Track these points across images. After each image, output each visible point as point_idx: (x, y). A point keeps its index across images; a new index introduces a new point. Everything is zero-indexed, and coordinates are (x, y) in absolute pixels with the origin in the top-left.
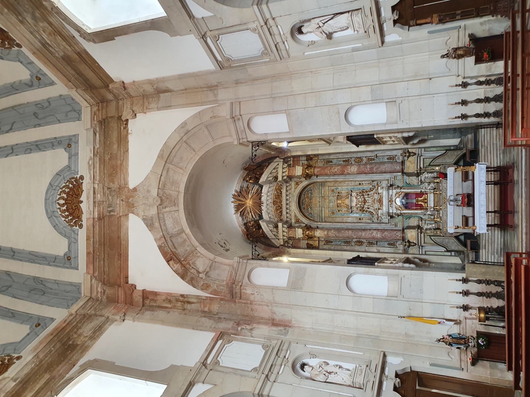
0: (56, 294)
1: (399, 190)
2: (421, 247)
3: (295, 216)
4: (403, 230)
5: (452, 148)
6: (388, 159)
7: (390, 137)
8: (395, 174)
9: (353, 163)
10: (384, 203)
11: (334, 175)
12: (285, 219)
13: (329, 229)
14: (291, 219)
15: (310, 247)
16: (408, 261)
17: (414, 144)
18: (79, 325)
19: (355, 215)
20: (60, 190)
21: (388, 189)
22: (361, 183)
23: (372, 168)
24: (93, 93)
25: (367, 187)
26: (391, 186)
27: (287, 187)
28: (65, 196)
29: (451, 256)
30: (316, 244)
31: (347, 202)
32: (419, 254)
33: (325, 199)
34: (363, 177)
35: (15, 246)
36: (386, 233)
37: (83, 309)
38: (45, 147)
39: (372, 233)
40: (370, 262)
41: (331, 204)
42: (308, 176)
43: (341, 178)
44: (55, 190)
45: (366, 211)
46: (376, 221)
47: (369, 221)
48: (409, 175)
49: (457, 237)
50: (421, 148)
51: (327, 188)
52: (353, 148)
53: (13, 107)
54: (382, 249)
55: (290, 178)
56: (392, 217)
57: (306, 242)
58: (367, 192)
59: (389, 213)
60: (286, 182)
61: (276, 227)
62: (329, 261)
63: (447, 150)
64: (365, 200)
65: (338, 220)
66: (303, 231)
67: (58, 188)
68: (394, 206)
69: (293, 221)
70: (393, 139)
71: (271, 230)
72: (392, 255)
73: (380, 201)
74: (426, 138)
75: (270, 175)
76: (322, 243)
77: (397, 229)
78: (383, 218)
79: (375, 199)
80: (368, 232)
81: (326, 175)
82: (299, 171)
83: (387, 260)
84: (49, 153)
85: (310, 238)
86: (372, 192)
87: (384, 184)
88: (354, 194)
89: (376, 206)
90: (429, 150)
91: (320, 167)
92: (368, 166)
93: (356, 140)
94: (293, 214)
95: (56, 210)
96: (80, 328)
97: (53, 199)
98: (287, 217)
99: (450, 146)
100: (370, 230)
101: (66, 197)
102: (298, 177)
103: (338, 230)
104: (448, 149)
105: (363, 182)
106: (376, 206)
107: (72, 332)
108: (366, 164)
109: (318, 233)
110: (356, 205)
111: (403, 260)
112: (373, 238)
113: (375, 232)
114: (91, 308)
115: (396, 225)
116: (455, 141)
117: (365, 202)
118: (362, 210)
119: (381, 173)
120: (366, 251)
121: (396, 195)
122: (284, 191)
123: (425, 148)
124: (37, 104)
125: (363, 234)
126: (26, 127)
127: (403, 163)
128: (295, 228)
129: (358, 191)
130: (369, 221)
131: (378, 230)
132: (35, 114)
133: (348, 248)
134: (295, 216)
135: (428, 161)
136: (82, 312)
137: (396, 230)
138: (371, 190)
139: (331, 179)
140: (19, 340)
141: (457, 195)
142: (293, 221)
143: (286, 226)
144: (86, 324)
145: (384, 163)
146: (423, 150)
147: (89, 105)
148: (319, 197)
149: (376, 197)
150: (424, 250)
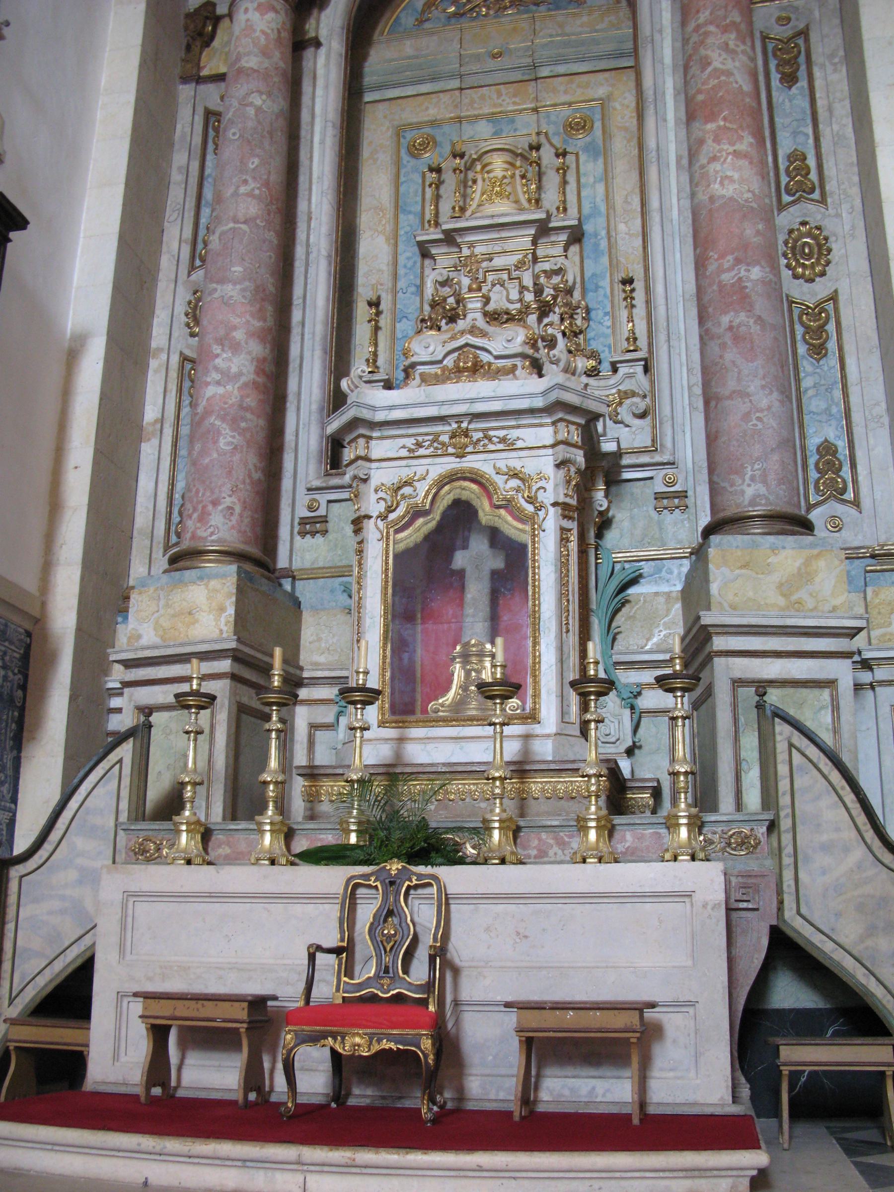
1: (552, 488)
21: (557, 408)
23: (739, 296)
25: (607, 332)
39: (235, 348)
41: (483, 129)
65: (376, 185)
68: (419, 467)
77: (284, 531)
92: (756, 273)
115: (313, 526)
119: (706, 371)
141: (440, 952)
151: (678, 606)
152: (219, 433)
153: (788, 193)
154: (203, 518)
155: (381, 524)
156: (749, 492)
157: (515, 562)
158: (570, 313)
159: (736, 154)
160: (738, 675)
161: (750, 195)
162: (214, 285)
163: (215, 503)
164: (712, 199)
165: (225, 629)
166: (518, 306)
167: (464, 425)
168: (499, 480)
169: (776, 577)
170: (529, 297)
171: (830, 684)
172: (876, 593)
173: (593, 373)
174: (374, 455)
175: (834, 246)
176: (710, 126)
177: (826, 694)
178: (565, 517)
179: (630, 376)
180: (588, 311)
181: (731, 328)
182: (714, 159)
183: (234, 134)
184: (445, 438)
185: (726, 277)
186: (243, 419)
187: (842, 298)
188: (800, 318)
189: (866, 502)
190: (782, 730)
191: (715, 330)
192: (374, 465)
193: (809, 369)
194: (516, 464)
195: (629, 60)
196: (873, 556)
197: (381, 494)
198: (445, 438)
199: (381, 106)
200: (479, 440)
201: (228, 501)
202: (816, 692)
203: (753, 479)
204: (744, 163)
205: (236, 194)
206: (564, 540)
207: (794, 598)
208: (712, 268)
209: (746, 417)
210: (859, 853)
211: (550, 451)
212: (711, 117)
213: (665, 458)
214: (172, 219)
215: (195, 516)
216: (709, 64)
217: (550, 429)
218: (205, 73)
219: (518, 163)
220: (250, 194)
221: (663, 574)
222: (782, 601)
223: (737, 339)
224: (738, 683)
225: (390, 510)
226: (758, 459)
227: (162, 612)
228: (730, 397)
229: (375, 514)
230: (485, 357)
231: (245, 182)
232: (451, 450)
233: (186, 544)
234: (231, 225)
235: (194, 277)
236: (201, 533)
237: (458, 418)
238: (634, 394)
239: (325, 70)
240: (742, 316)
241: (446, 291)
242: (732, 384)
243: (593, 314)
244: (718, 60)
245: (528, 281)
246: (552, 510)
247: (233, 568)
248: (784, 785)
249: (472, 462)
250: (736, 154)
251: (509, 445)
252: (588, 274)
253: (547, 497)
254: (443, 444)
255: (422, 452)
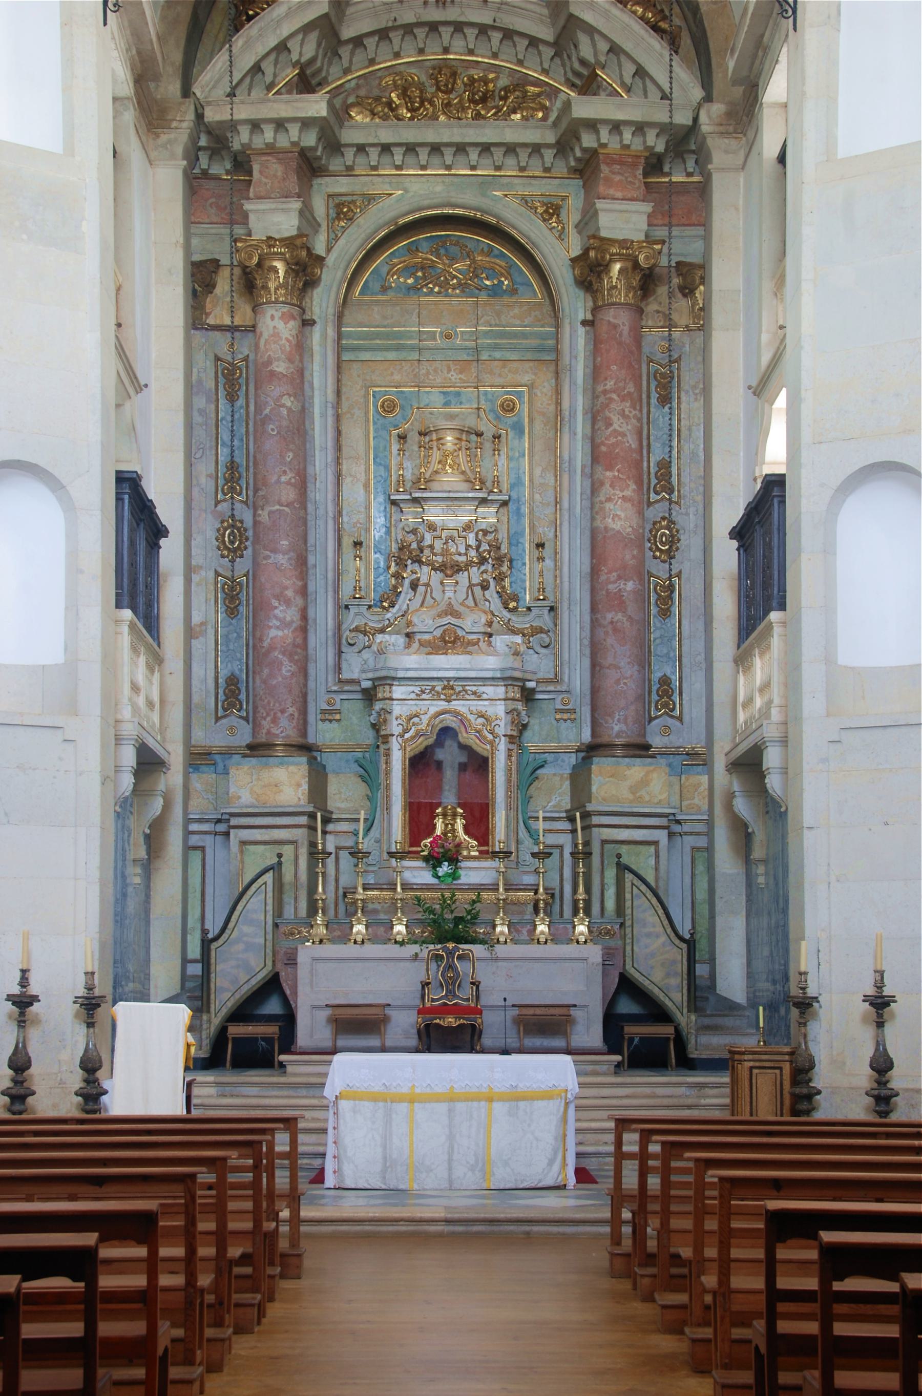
1: (503, 727)
2: (221, 827)
3: (370, 199)
4: (306, 749)
5: (701, 970)
6: (665, 681)
7: (766, 686)
8: (586, 712)
9: (655, 512)
10: (440, 660)
11: (595, 416)
12: (349, 136)
13: (299, 381)
14: (349, 171)
15: (201, 277)
16: (148, 763)
17: (730, 797)
19: (378, 520)
21: (508, 680)
22: (547, 552)
23: (618, 601)
26: (528, 696)
27: (536, 149)
29: (185, 961)
30: (219, 315)
31: (450, 480)
32: (187, 821)
33: (464, 366)
34: (574, 556)
36: (287, 668)
39: (288, 602)
40: (136, 586)
41: (435, 397)
42: (590, 270)
43: (576, 450)
45: (397, 576)
46: (352, 620)
47: (347, 590)
48: (580, 780)
49: (272, 985)
50: (710, 834)
51: (527, 378)
52: (728, 511)
54: (203, 646)
55: (587, 169)
56: (369, 696)
57: (225, 260)
58: (499, 579)
59: (388, 680)
60: (562, 147)
61: (306, 83)
62: (130, 380)
63: (691, 944)
64: (457, 569)
65: (354, 434)
66: (288, 242)
69: (341, 185)
70: (758, 702)
71: (282, 47)
72: (176, 695)
73: (449, 642)
74: (758, 852)
75: (603, 46)
76: (221, 341)
77: (311, 718)
78: (366, 654)
79: (457, 615)
80: (290, 583)
81: (596, 374)
82: (624, 219)
83: (151, 669)
85: (250, 283)
86: (496, 604)
87: (539, 665)
88: (488, 516)
89: (426, 622)
90: (701, 868)
91: (638, 339)
92: (630, 586)
93: (764, 518)
94: (377, 187)
98: (361, 149)
99: (712, 961)
100: (303, 591)
102: (589, 216)
103: (299, 430)
104: (695, 949)
105: (549, 563)
106: (426, 622)
108: (642, 574)
109: (276, 325)
110: (432, 527)
111: (151, 743)
112: (260, 610)
113: (291, 614)
115: (329, 715)
116: (732, 979)
117: (450, 569)
118: (407, 555)
120: (189, 570)
121: (481, 715)
122: (516, 129)
123: (709, 849)
125: (282, 560)
127: (640, 749)
128: (304, 194)
129: (502, 535)
130: (347, 590)
131: (304, 630)
133: (204, 481)
134: (370, 199)
135: (643, 861)
137: (304, 712)
138: (508, 600)
139: (577, 402)
141: (476, 984)
142: (341, 185)
143: (310, 139)
145: (644, 660)
146: (702, 842)
148: (476, 336)
149: (472, 623)
150: (208, 841)
151: (568, 783)
152: (282, 664)
153: (657, 493)
154: (275, 721)
155: (400, 740)
156: (616, 728)
157: (478, 765)
158: (499, 560)
159: (624, 498)
160: (604, 837)
161: (630, 529)
162: (268, 553)
163: (283, 711)
164: (606, 528)
165: (302, 797)
166: (463, 559)
167: (451, 683)
168: (472, 718)
169: (628, 783)
170: (473, 553)
171: (656, 843)
172: (687, 779)
173: (514, 610)
174: (395, 696)
175: (682, 537)
176: (608, 474)
177: (652, 849)
178: (510, 743)
179: (539, 616)
180: (511, 561)
181: (612, 623)
182: (609, 500)
183: (273, 430)
184: (438, 688)
185: (611, 587)
186: (296, 653)
187: (683, 576)
188: (655, 589)
189: (686, 718)
190: (629, 876)
191: (602, 621)
192: (395, 702)
193: (658, 625)
194: (479, 708)
195: (551, 356)
196: (687, 754)
197: (399, 721)
198: (438, 688)
199: (355, 365)
200: (460, 692)
201: (291, 710)
202: (647, 847)
203: (619, 720)
204: (628, 505)
205: (278, 481)
206: (509, 756)
207: (638, 794)
208: (603, 577)
209: (618, 682)
210: (663, 939)
211: (503, 702)
212: (610, 468)
213: (564, 688)
214: (198, 456)
215: (269, 719)
216: (611, 425)
217: (503, 689)
218: (211, 321)
219: (464, 437)
220: (288, 483)
221: (559, 762)
222: (631, 797)
223: (615, 630)
224: (604, 842)
225: (406, 731)
226: (623, 709)
227: (254, 782)
228: (608, 668)
229: (396, 734)
230: (460, 633)
231: (285, 472)
232: (442, 697)
233: (262, 738)
234: (277, 507)
235: (219, 507)
236: (275, 731)
237: (449, 679)
238: (541, 630)
239: (320, 340)
240: (620, 616)
241: (411, 537)
242: (610, 660)
243: (514, 563)
244: (618, 423)
245: (472, 541)
246: (503, 738)
247: (304, 759)
248: (628, 904)
249: (457, 705)
250: (624, 498)
251: (478, 696)
252: (512, 532)
253: (501, 731)
254: (438, 693)
255: (424, 696)
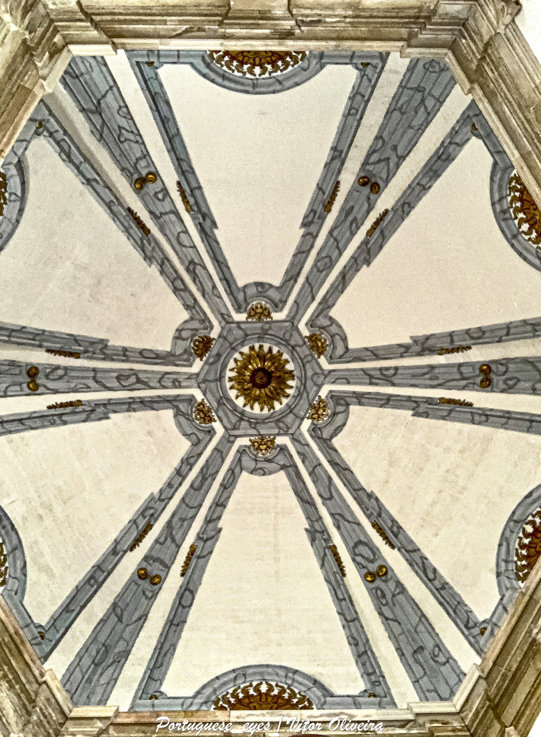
0: (89, 681)
18: (17, 687)
20: (286, 686)
24: (486, 712)
28: (276, 692)
35: (187, 627)
37: (48, 700)
38: (364, 664)
44: (286, 676)
53: (424, 615)
67: (289, 682)
84: (354, 670)
95: (248, 679)
96: (11, 687)
97: (269, 674)
101: (272, 694)
107: (9, 670)
114: (45, 717)
124: (439, 646)
126: (393, 637)
132: (422, 648)
136: (41, 700)
140: (25, 603)
144: (16, 700)
147: (458, 708)
